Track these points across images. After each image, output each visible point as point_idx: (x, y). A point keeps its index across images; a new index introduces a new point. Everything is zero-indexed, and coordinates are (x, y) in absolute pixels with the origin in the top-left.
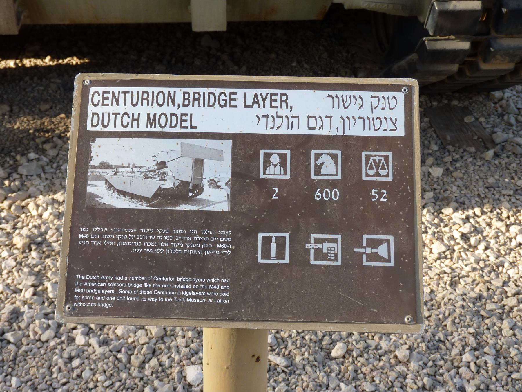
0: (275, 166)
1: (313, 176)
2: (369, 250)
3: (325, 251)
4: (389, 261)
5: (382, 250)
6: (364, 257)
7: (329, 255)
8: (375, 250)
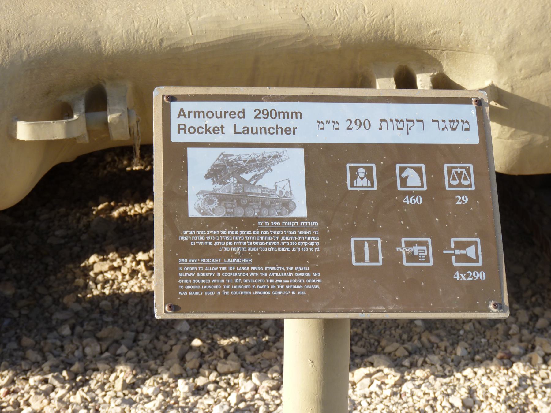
2: (457, 252)
3: (416, 253)
5: (470, 252)
6: (454, 258)
7: (420, 257)
8: (463, 252)
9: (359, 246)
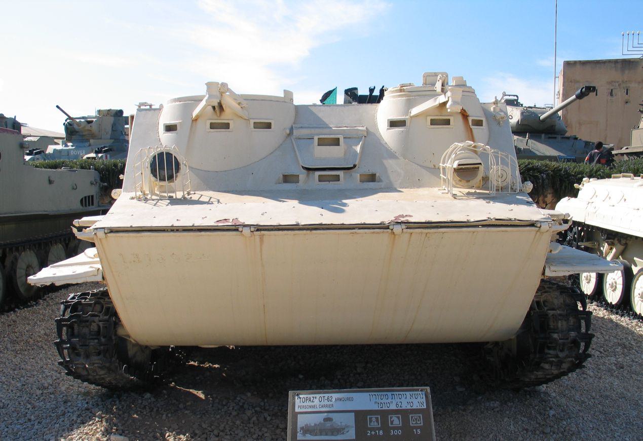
0: (374, 422)
1: (390, 425)
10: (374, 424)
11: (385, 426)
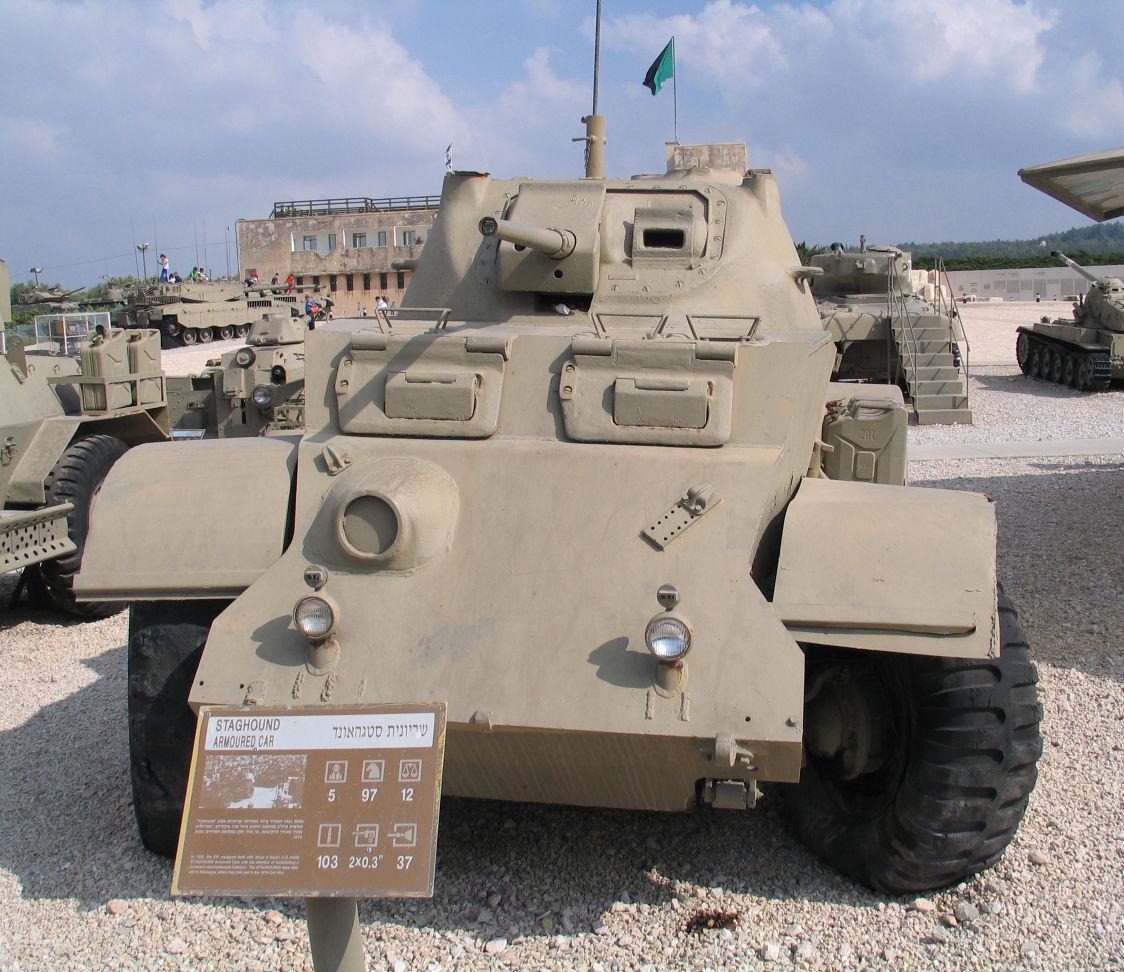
0: (336, 773)
4: (412, 842)
5: (408, 835)
6: (394, 840)
9: (325, 830)
10: (336, 778)
11: (353, 786)
